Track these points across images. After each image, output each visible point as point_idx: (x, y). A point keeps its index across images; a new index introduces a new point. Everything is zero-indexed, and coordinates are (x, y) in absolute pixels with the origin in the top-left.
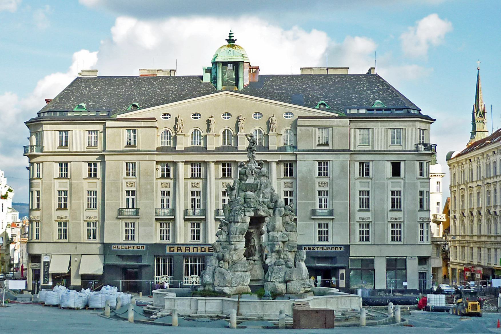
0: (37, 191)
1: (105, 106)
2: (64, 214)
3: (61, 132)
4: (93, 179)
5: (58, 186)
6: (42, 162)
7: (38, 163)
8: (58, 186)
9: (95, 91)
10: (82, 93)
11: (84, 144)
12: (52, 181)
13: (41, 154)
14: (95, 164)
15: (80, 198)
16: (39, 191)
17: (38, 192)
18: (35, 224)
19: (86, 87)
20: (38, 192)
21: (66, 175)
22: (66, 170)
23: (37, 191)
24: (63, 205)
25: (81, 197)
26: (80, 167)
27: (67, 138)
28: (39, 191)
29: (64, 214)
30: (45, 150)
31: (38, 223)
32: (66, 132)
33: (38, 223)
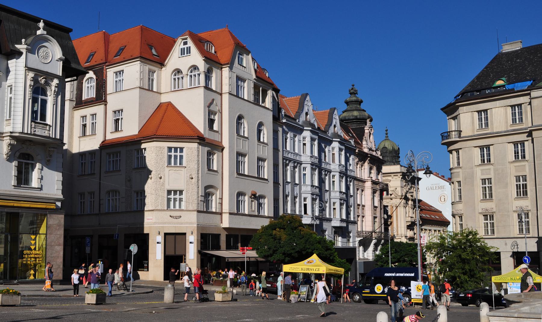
0: (458, 182)
1: (529, 76)
2: (489, 206)
3: (479, 112)
4: (520, 161)
5: (479, 173)
6: (461, 149)
7: (457, 151)
8: (480, 174)
9: (518, 62)
10: (503, 67)
11: (507, 122)
12: (472, 168)
13: (458, 139)
14: (522, 143)
15: (506, 186)
16: (460, 182)
17: (459, 182)
18: (457, 218)
19: (507, 61)
20: (459, 182)
21: (489, 160)
22: (489, 155)
23: (458, 182)
24: (488, 194)
25: (507, 184)
26: (504, 150)
27: (486, 119)
28: (460, 182)
29: (489, 206)
30: (463, 135)
31: (461, 217)
32: (486, 111)
33: (461, 217)
